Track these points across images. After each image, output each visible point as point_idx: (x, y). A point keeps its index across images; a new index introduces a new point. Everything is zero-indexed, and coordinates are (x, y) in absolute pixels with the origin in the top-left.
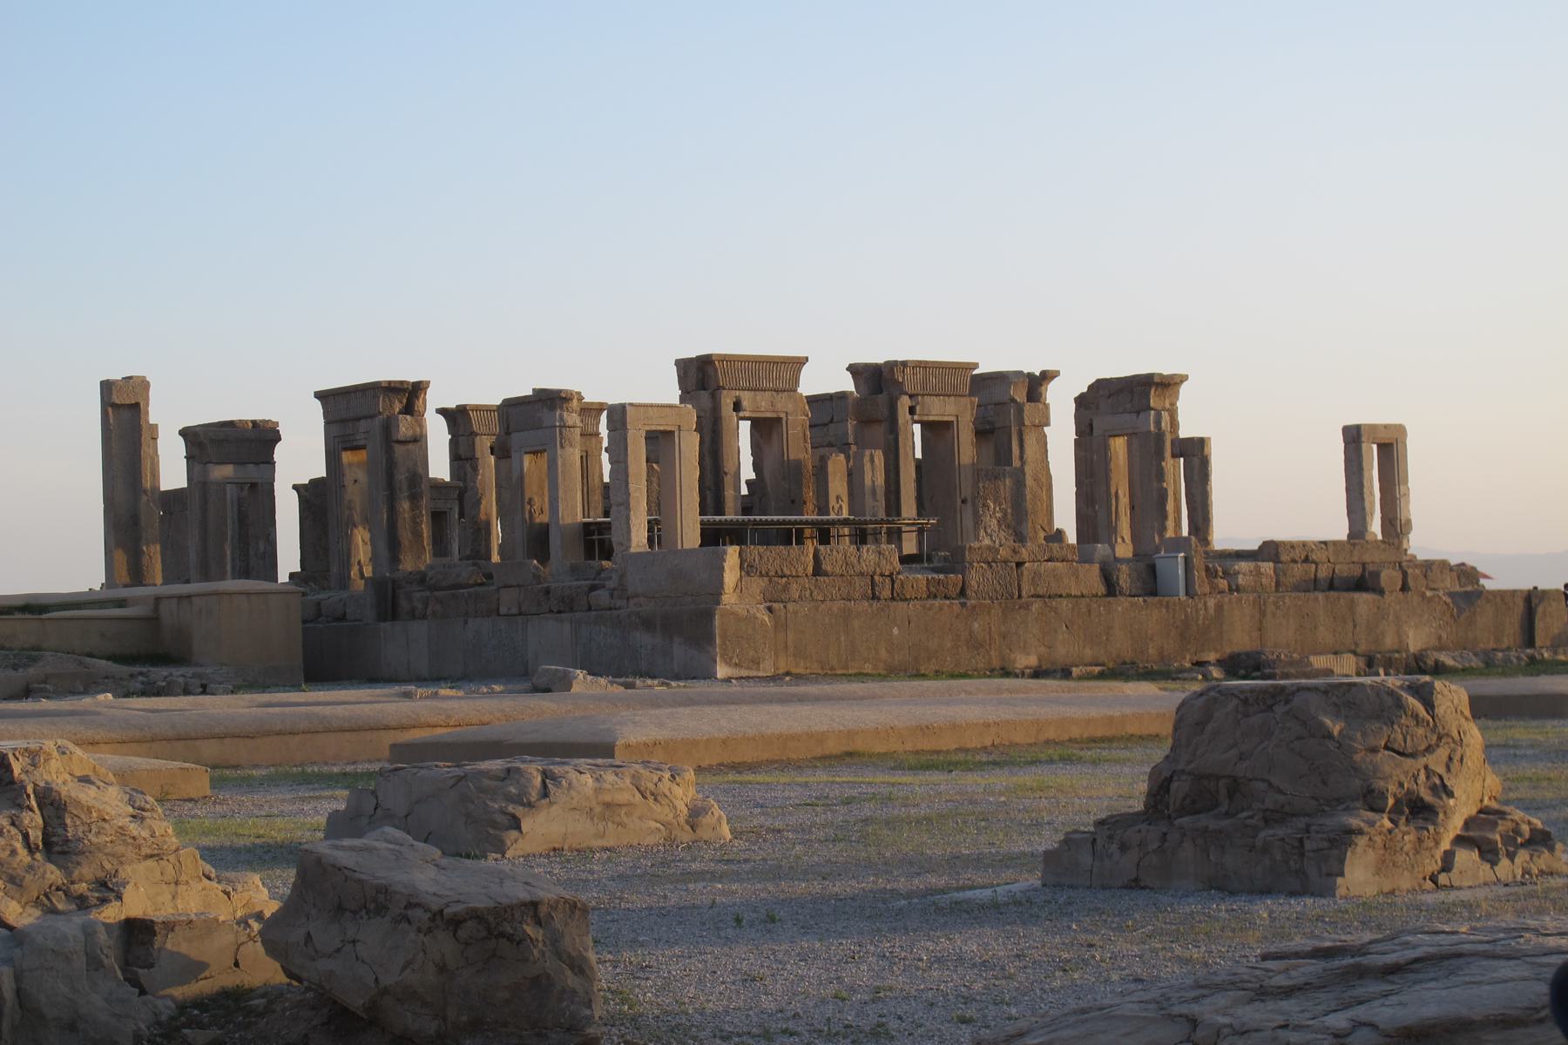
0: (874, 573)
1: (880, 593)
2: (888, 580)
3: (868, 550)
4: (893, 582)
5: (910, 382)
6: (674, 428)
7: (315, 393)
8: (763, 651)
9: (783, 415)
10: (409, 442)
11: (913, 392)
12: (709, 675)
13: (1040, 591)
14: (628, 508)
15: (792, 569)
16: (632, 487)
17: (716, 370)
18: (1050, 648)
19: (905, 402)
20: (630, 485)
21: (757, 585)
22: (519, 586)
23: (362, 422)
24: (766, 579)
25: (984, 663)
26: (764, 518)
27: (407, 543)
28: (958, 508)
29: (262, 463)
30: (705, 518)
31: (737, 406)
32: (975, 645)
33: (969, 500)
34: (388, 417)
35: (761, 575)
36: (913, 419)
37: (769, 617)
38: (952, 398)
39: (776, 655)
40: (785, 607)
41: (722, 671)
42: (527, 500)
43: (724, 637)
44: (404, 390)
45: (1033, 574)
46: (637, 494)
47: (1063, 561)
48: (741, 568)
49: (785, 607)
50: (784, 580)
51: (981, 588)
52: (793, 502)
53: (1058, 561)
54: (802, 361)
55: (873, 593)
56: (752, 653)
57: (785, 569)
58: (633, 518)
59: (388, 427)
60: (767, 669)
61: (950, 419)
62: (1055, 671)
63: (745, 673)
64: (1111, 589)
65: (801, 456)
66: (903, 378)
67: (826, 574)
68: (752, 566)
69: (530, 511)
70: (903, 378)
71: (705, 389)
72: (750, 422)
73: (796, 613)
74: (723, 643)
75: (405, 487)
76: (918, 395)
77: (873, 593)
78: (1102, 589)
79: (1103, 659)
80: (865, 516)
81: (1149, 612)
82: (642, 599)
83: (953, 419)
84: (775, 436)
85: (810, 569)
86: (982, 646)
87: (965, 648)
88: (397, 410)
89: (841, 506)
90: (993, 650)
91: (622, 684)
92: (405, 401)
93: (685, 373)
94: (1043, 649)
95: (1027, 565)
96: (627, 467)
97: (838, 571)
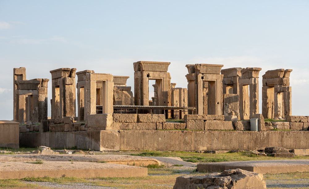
0: (157, 122)
1: (158, 128)
2: (161, 124)
3: (155, 116)
4: (163, 125)
5: (202, 70)
6: (106, 80)
7: (50, 71)
8: (116, 144)
9: (162, 78)
10: (70, 84)
11: (203, 73)
12: (97, 149)
13: (211, 128)
14: (90, 103)
15: (130, 120)
16: (91, 97)
17: (142, 66)
18: (210, 145)
19: (200, 76)
20: (91, 96)
21: (118, 125)
22: (68, 123)
23: (59, 79)
24: (121, 123)
25: (189, 149)
26: (120, 106)
27: (68, 111)
28: (216, 105)
29: (34, 90)
30: (97, 106)
31: (148, 76)
32: (186, 143)
33: (220, 103)
34: (64, 78)
35: (120, 122)
36: (203, 80)
37: (118, 134)
38: (215, 75)
39: (121, 145)
40: (124, 131)
41: (102, 149)
42: (80, 100)
43: (103, 139)
44: (69, 71)
45: (209, 124)
46: (93, 98)
47: (219, 120)
48: (113, 120)
49: (124, 131)
50: (127, 123)
51: (192, 127)
52: (165, 102)
53: (217, 120)
54: (168, 64)
55: (156, 128)
56: (112, 144)
57: (127, 121)
58: (91, 105)
59: (64, 81)
60: (117, 148)
61: (214, 80)
62: (211, 152)
63: (109, 150)
64: (235, 127)
65: (167, 90)
66: (200, 69)
67: (141, 122)
68: (117, 119)
69: (81, 103)
70: (200, 69)
71: (140, 71)
72: (155, 80)
73: (127, 133)
74: (103, 141)
75: (68, 97)
76: (204, 74)
77: (156, 128)
78: (233, 128)
79: (229, 148)
80: (168, 106)
81: (244, 135)
82: (90, 128)
83: (216, 80)
84: (161, 84)
85: (136, 121)
86: (188, 144)
87: (183, 144)
88: (67, 76)
89: (177, 104)
90: (192, 145)
91: (59, 152)
92: (69, 73)
93: (135, 66)
94: (209, 145)
95: (207, 121)
96: (90, 91)
97: (145, 121)
